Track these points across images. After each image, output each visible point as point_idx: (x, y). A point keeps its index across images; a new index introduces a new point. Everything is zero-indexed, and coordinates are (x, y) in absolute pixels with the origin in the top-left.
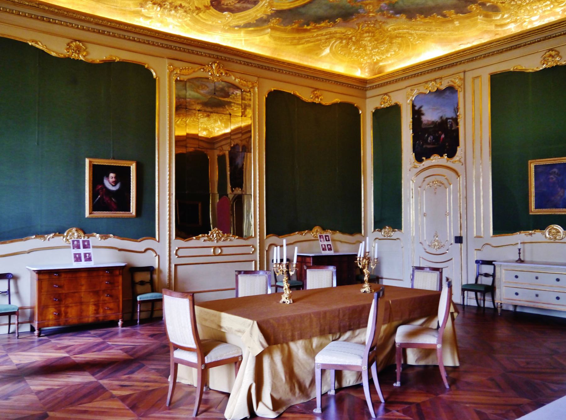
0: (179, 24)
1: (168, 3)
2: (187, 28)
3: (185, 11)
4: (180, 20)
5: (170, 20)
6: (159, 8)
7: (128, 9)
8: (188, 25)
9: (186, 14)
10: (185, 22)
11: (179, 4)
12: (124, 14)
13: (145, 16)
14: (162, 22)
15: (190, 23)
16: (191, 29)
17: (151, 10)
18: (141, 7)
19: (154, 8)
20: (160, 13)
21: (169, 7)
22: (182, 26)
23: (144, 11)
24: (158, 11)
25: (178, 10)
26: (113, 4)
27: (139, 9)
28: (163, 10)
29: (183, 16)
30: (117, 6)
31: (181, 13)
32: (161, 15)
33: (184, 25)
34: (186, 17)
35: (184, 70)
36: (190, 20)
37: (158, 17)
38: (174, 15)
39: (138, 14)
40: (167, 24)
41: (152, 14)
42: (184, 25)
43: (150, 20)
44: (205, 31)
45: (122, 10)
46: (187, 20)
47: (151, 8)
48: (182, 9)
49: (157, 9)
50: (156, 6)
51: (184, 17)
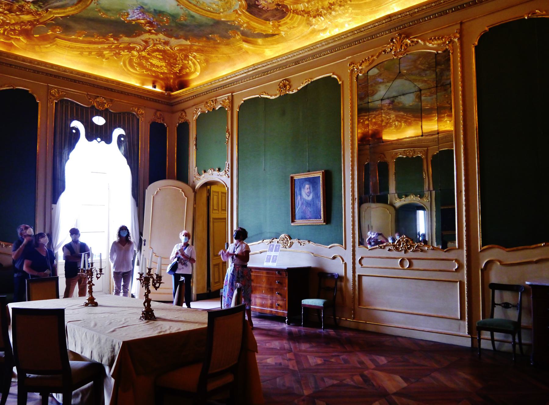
0: (350, 19)
1: (321, 10)
2: (359, 17)
3: (340, 6)
4: (347, 15)
5: (340, 20)
6: (321, 18)
7: (305, 33)
8: (357, 14)
9: (344, 7)
10: (352, 13)
11: (329, 4)
12: (307, 38)
13: (321, 30)
14: (337, 26)
15: (357, 11)
16: (363, 15)
17: (319, 23)
18: (311, 26)
19: (318, 20)
20: (327, 21)
21: (325, 12)
22: (354, 18)
23: (316, 27)
24: (324, 20)
25: (334, 9)
26: (295, 37)
27: (311, 28)
28: (326, 17)
29: (343, 10)
30: (298, 36)
31: (339, 9)
32: (330, 21)
33: (354, 16)
34: (348, 9)
35: (365, 62)
36: (353, 9)
37: (329, 24)
38: (338, 15)
39: (314, 32)
40: (342, 25)
41: (324, 26)
42: (354, 16)
43: (328, 31)
44: (377, 9)
45: (303, 37)
46: (351, 11)
47: (317, 21)
48: (336, 6)
49: (321, 19)
50: (317, 17)
51: (346, 11)
